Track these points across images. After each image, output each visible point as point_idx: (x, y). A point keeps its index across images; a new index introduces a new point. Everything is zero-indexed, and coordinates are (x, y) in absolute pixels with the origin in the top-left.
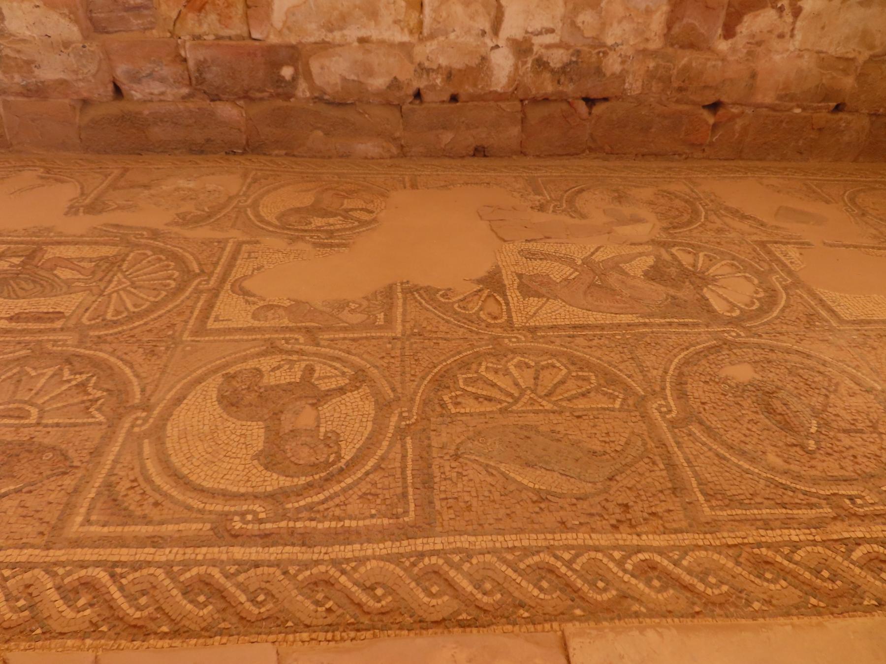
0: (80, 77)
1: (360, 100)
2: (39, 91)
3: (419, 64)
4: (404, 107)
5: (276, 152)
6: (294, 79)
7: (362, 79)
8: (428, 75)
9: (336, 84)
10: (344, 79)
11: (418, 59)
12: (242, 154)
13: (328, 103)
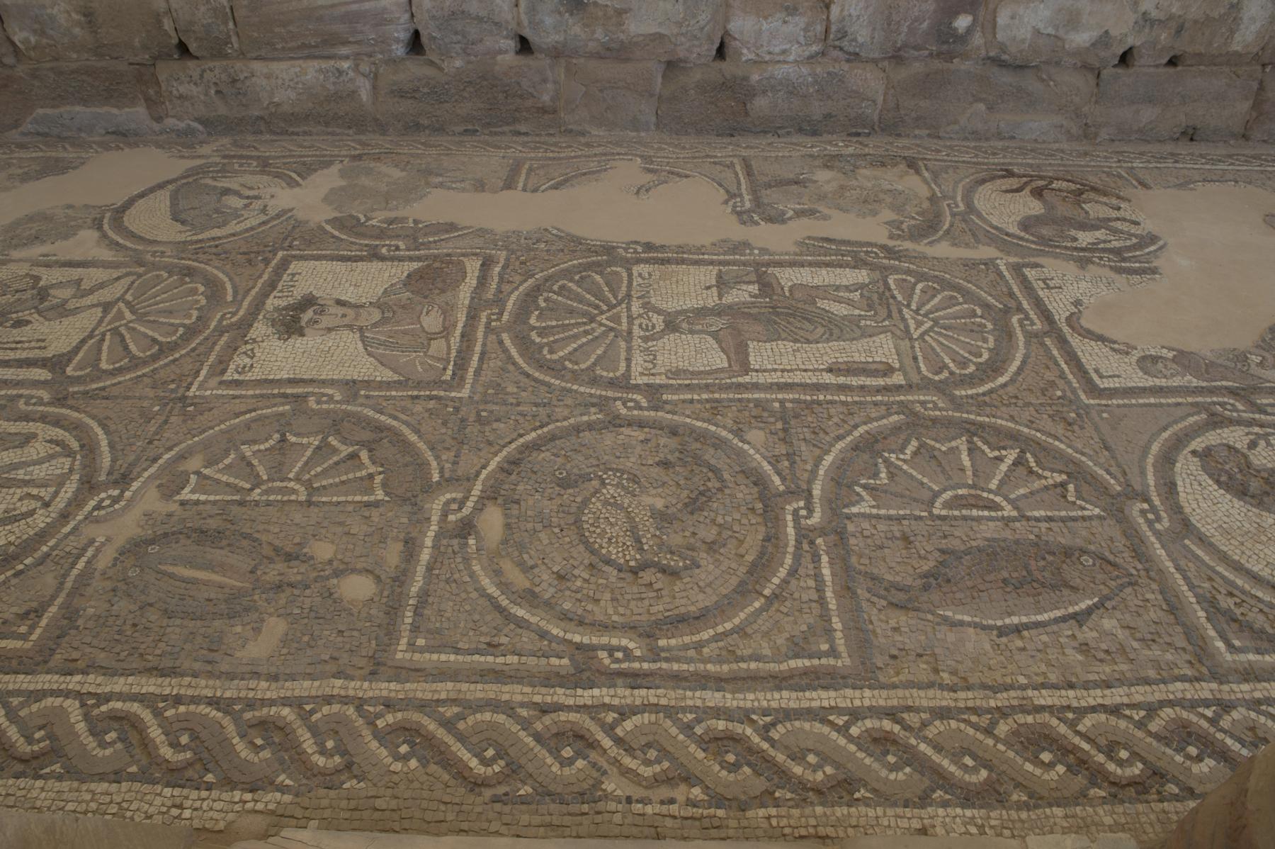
0: (684, 30)
1: (1047, 63)
2: (619, 52)
3: (1144, 13)
4: (1105, 73)
5: (917, 132)
6: (969, 31)
7: (1061, 33)
8: (1152, 26)
9: (1023, 41)
10: (1037, 32)
11: (1143, 8)
13: (1002, 64)
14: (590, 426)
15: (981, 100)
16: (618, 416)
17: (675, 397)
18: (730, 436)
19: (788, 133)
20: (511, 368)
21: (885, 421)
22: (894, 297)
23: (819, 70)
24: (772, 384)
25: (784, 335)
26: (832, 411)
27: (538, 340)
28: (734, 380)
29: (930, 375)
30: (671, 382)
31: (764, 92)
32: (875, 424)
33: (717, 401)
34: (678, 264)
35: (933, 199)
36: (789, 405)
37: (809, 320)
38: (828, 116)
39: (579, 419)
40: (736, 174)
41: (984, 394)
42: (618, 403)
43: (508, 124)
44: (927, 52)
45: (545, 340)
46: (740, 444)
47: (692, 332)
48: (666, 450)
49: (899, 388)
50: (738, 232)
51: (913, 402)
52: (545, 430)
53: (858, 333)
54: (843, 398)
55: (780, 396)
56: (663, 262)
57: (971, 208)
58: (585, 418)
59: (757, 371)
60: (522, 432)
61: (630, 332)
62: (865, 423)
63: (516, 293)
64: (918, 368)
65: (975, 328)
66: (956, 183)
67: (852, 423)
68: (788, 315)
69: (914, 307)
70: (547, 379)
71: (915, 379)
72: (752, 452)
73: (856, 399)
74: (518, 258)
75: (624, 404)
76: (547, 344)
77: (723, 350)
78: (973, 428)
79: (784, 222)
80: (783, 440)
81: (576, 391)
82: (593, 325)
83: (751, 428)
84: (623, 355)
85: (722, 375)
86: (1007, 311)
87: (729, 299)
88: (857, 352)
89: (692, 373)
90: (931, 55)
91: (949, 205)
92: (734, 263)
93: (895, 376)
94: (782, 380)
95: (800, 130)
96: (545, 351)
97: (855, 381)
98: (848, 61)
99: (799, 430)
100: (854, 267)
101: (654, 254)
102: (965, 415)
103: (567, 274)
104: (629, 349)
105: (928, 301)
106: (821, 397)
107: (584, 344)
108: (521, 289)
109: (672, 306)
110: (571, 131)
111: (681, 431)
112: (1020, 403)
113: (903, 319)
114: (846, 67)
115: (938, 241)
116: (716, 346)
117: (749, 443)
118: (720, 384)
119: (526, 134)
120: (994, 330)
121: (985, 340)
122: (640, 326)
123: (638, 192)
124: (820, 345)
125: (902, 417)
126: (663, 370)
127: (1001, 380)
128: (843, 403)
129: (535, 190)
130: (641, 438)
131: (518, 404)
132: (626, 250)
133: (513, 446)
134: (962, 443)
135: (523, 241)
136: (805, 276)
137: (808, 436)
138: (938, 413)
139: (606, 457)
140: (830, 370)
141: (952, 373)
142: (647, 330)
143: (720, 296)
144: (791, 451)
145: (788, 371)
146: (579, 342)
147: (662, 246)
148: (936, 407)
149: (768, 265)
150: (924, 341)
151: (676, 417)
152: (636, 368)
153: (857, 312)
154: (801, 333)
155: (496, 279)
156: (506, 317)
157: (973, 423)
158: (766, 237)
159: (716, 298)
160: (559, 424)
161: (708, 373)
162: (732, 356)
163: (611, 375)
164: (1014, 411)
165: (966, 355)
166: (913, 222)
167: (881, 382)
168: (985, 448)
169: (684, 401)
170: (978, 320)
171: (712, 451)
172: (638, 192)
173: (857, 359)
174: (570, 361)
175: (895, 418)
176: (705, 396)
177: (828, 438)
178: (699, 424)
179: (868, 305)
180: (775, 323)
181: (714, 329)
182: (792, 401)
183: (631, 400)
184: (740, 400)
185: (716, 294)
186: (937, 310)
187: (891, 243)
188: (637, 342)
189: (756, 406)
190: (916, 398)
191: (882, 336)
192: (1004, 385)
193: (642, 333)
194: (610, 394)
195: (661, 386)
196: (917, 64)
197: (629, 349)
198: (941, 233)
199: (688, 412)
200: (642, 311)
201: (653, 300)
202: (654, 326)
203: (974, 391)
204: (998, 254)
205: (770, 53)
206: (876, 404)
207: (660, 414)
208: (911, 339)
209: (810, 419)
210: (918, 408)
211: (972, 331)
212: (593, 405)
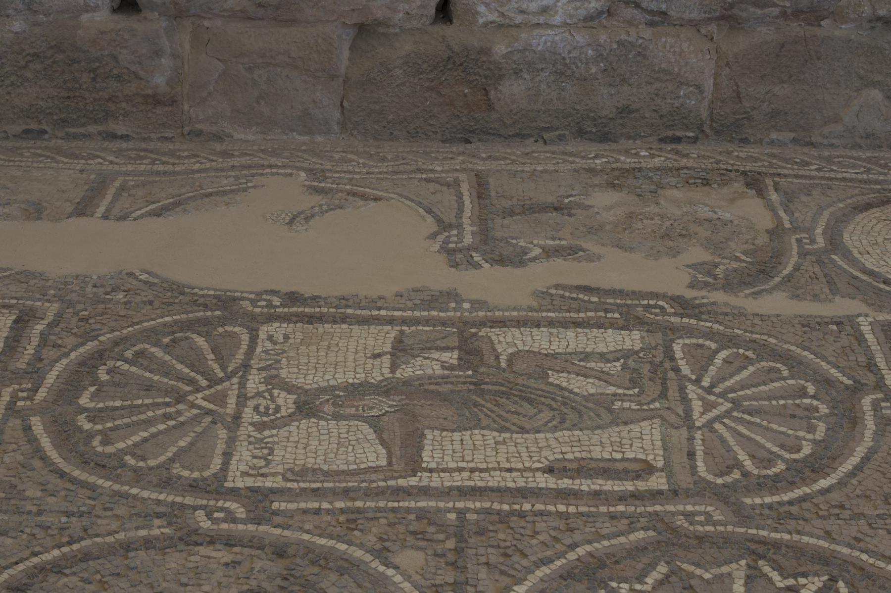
5: (774, 136)
12: (695, 140)
14: (148, 544)
15: (874, 84)
16: (196, 532)
17: (292, 506)
18: (368, 558)
19: (561, 138)
20: (37, 463)
21: (622, 539)
22: (676, 370)
23: (603, 38)
24: (451, 488)
25: (485, 422)
26: (541, 526)
27: (87, 426)
28: (391, 483)
29: (710, 478)
30: (289, 485)
31: (517, 72)
32: (606, 543)
33: (358, 511)
34: (335, 322)
35: (776, 233)
36: (471, 516)
37: (530, 401)
38: (625, 111)
39: (131, 534)
40: (460, 196)
41: (790, 503)
42: (200, 514)
43: (96, 122)
44: (776, 11)
45: (99, 427)
46: (382, 568)
47: (337, 417)
48: (262, 576)
49: (655, 495)
50: (439, 276)
51: (673, 514)
52: (75, 547)
53: (606, 417)
54: (562, 508)
55: (460, 505)
56: (311, 319)
57: (835, 243)
58: (143, 533)
59: (431, 471)
60: (37, 549)
61: (237, 417)
62: (589, 542)
63: (65, 361)
64: (693, 469)
65: (799, 412)
66: (821, 209)
67: (568, 541)
68: (492, 391)
69: (706, 383)
70: (92, 479)
71: (685, 480)
72: (398, 578)
74: (76, 314)
75: (209, 515)
76: (99, 432)
77: (383, 442)
78: (761, 549)
79: (522, 263)
80: (453, 564)
81: (135, 497)
82: (181, 407)
83: (404, 547)
84: (221, 447)
85: (374, 477)
86: (858, 389)
87: (406, 372)
88: (599, 445)
89: (327, 473)
90: (784, 14)
91: (799, 241)
92: (427, 322)
93: (653, 478)
95: (581, 133)
96: (96, 442)
97: (585, 485)
98: (651, 24)
99: (481, 551)
100: (622, 328)
101: (302, 309)
102: (753, 531)
103: (152, 336)
104: (232, 441)
105: (732, 375)
106: (527, 507)
107: (160, 432)
108: (73, 355)
109: (311, 380)
110: (200, 133)
111: (290, 551)
112: (846, 514)
113: (685, 400)
114: (647, 33)
115: (770, 291)
116: (372, 436)
117: (396, 568)
119: (125, 137)
120: (827, 416)
121: (811, 429)
122: (256, 408)
123: (291, 222)
124: (540, 436)
125: (651, 533)
126: (280, 469)
127: (823, 483)
128: (559, 514)
129: (123, 218)
130: (225, 560)
131: (39, 513)
132: (254, 303)
133: (21, 567)
134: (738, 570)
135: (89, 289)
136: (540, 340)
137: (493, 559)
138: (710, 528)
139: (164, 585)
140: (550, 470)
141: (746, 474)
142: (266, 414)
143: (394, 368)
144: (462, 578)
145: (481, 471)
146: (153, 430)
147: (314, 298)
149: (482, 324)
150: (713, 430)
151: (287, 533)
152: (237, 466)
153: (611, 390)
154: (515, 419)
155: (35, 341)
156: (41, 394)
157: (763, 542)
158: (493, 285)
160: (98, 540)
161: (353, 473)
162: (397, 451)
163: (196, 475)
164: (833, 525)
165: (775, 449)
166: (735, 265)
167: (629, 486)
168: (775, 576)
169: (305, 512)
170: (807, 401)
171: (333, 577)
172: (291, 222)
174: (133, 455)
175: (641, 534)
176: (340, 504)
177: (525, 562)
178: (322, 541)
179: (631, 380)
180: (476, 405)
181: (374, 412)
182: (477, 512)
183: (221, 509)
184: (394, 510)
186: (743, 388)
187: (689, 294)
188: (245, 430)
189: (418, 518)
190: (681, 508)
191: (645, 424)
192: (828, 490)
193: (257, 418)
194: (189, 500)
195: (272, 491)
196: (764, 29)
198: (777, 280)
199: (307, 527)
200: (262, 388)
201: (283, 373)
202: (278, 409)
203: (776, 498)
204: (864, 309)
205: (522, 12)
206: (613, 517)
207: (262, 528)
208: (691, 427)
209: (501, 536)
210: (680, 521)
211: (793, 416)
212: (159, 516)
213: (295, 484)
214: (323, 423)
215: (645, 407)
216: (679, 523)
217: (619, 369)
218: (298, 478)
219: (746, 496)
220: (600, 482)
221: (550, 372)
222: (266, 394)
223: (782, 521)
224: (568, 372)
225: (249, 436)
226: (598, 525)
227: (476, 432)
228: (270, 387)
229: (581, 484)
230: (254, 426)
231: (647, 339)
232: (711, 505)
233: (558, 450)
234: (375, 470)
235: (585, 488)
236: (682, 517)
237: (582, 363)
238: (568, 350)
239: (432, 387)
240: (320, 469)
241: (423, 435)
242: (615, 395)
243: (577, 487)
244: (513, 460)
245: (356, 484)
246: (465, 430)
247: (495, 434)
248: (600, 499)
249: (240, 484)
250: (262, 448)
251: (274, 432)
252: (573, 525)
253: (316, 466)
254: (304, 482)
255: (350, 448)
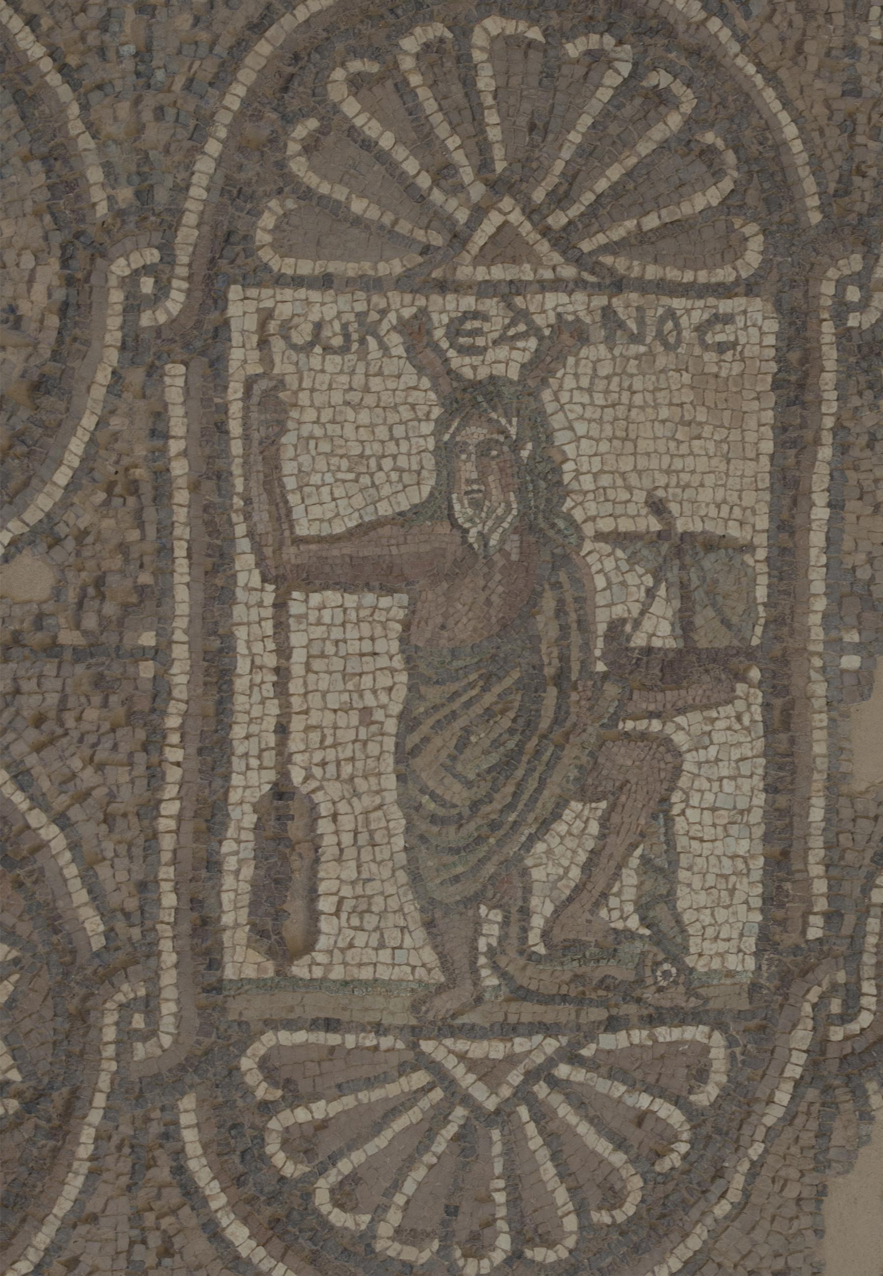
33: (162, 494)
41: (180, 1170)
51: (154, 979)
54: (171, 808)
59: (280, 605)
67: (76, 814)
73: (167, 843)
77: (363, 529)
82: (477, 191)
85: (262, 517)
94: (243, 666)
97: (238, 851)
102: (100, 1100)
104: (372, 285)
116: (384, 509)
118: (227, 509)
125: (97, 943)
140: (281, 792)
148: (126, 1038)
152: (286, 303)
157: (71, 1110)
159: (606, 525)
161: (272, 479)
173: (327, 870)
180: (488, 680)
185: (625, 525)
188: (404, 306)
194: (187, 235)
197: (372, 285)
206: (146, 887)
213: (240, 395)
214: (427, 428)
215: (482, 960)
216: (125, 987)
217: (619, 925)
218: (255, 399)
219: (200, 1102)
220: (248, 872)
221: (603, 805)
222: (522, 328)
223: (127, 1150)
224: (602, 836)
225: (383, 312)
226: (122, 863)
227: (403, 678)
228: (547, 332)
229: (238, 841)
230: (415, 317)
231: (728, 981)
232: (175, 1042)
233: (343, 807)
234: (282, 514)
235: (228, 846)
236: (142, 992)
237: (634, 862)
238: (682, 842)
239: (549, 603)
240: (284, 431)
241: (391, 592)
242: (525, 913)
243: (231, 832)
244: (315, 737)
245: (240, 488)
246: (408, 660)
247: (396, 709)
248: (194, 869)
249: (234, 310)
250: (347, 336)
251: (400, 351)
252: (120, 823)
253: (291, 425)
254: (246, 409)
255: (351, 476)
